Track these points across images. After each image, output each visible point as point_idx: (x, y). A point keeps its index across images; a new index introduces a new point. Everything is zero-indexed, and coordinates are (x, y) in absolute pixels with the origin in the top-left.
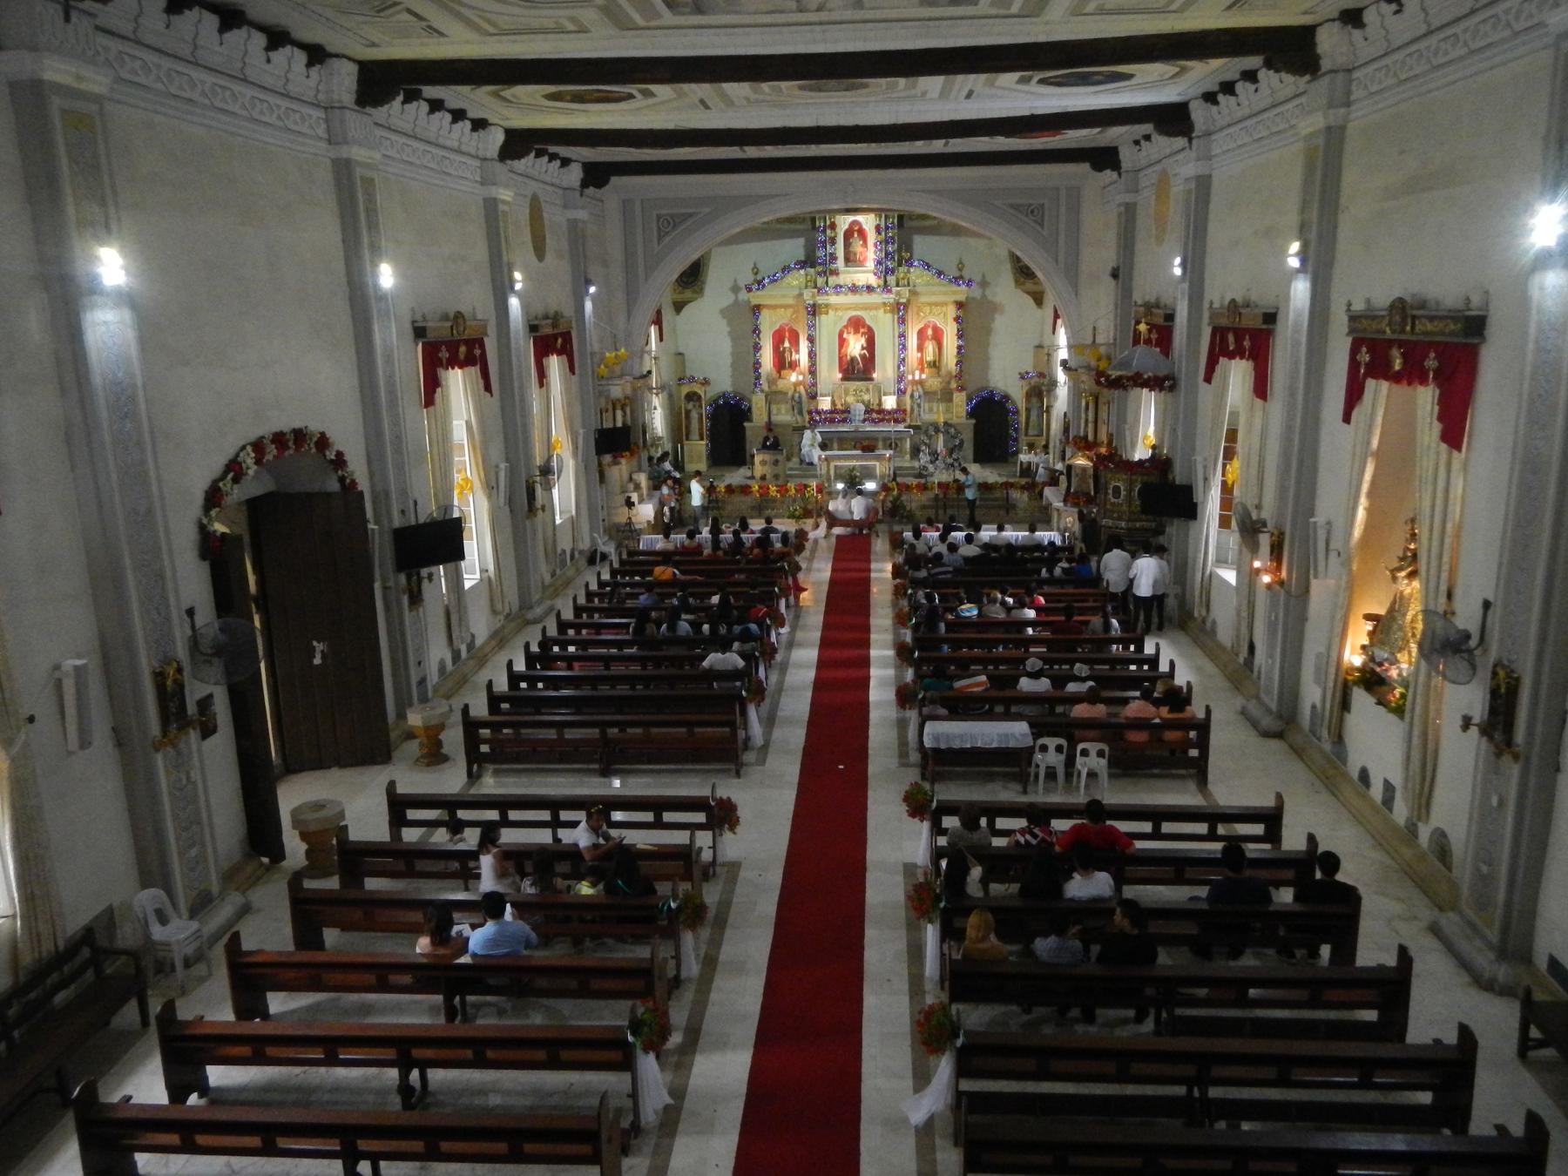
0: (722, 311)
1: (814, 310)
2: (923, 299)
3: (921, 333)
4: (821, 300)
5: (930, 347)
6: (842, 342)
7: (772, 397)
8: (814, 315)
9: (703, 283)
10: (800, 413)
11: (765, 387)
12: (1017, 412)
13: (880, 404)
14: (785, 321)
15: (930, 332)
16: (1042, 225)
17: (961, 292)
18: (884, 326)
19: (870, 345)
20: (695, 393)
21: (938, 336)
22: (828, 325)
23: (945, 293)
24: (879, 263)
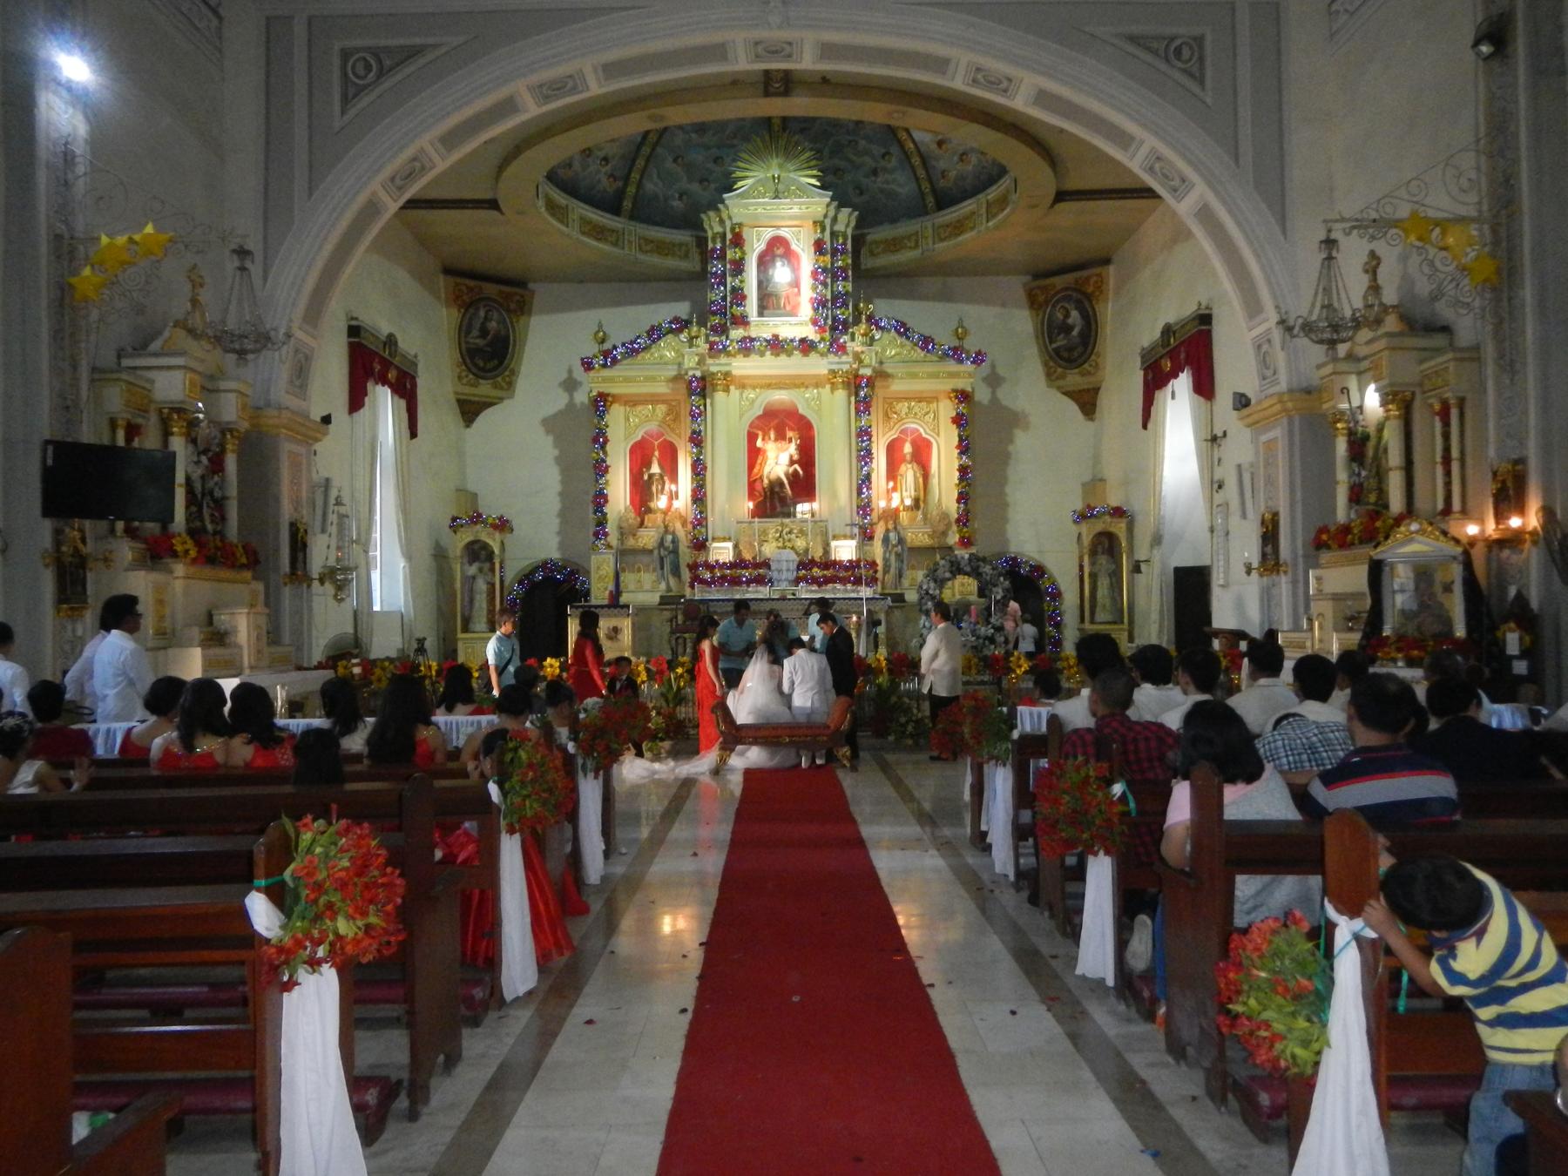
0: (550, 424)
1: (702, 387)
2: (897, 386)
3: (893, 449)
4: (716, 366)
5: (909, 473)
6: (754, 454)
7: (627, 557)
8: (703, 394)
9: (513, 373)
10: (676, 571)
11: (613, 539)
12: (1057, 595)
13: (827, 551)
14: (653, 426)
15: (908, 448)
16: (1201, 82)
17: (964, 375)
18: (831, 414)
19: (806, 456)
20: (485, 546)
21: (921, 456)
22: (729, 415)
23: (935, 376)
24: (820, 304)
